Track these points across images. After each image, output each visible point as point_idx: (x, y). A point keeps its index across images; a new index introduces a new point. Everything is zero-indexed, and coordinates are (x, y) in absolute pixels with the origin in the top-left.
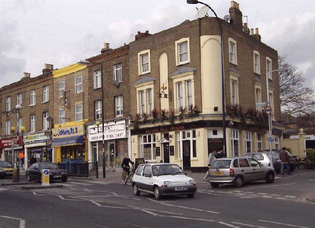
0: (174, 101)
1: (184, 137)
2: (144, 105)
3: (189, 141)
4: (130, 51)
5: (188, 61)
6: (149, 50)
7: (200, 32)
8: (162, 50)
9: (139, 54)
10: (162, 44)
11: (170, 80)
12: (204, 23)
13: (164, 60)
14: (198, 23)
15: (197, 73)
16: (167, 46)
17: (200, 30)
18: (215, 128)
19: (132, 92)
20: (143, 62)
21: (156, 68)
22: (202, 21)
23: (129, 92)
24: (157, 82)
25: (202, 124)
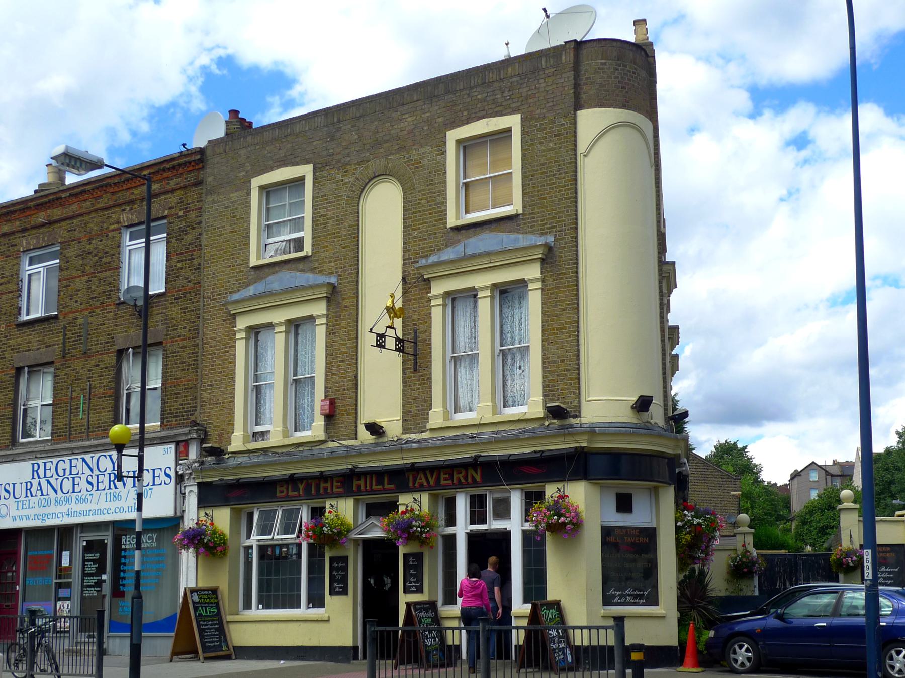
0: (428, 365)
1: (477, 516)
2: (271, 408)
3: (505, 536)
4: (210, 176)
5: (515, 207)
6: (310, 167)
7: (577, 96)
8: (375, 165)
9: (257, 182)
10: (378, 144)
11: (415, 283)
12: (590, 63)
13: (383, 211)
14: (567, 58)
15: (560, 265)
16: (401, 149)
17: (576, 86)
18: (625, 486)
19: (212, 331)
20: (273, 229)
21: (340, 237)
22: (584, 51)
23: (196, 331)
24: (342, 299)
25: (576, 465)
